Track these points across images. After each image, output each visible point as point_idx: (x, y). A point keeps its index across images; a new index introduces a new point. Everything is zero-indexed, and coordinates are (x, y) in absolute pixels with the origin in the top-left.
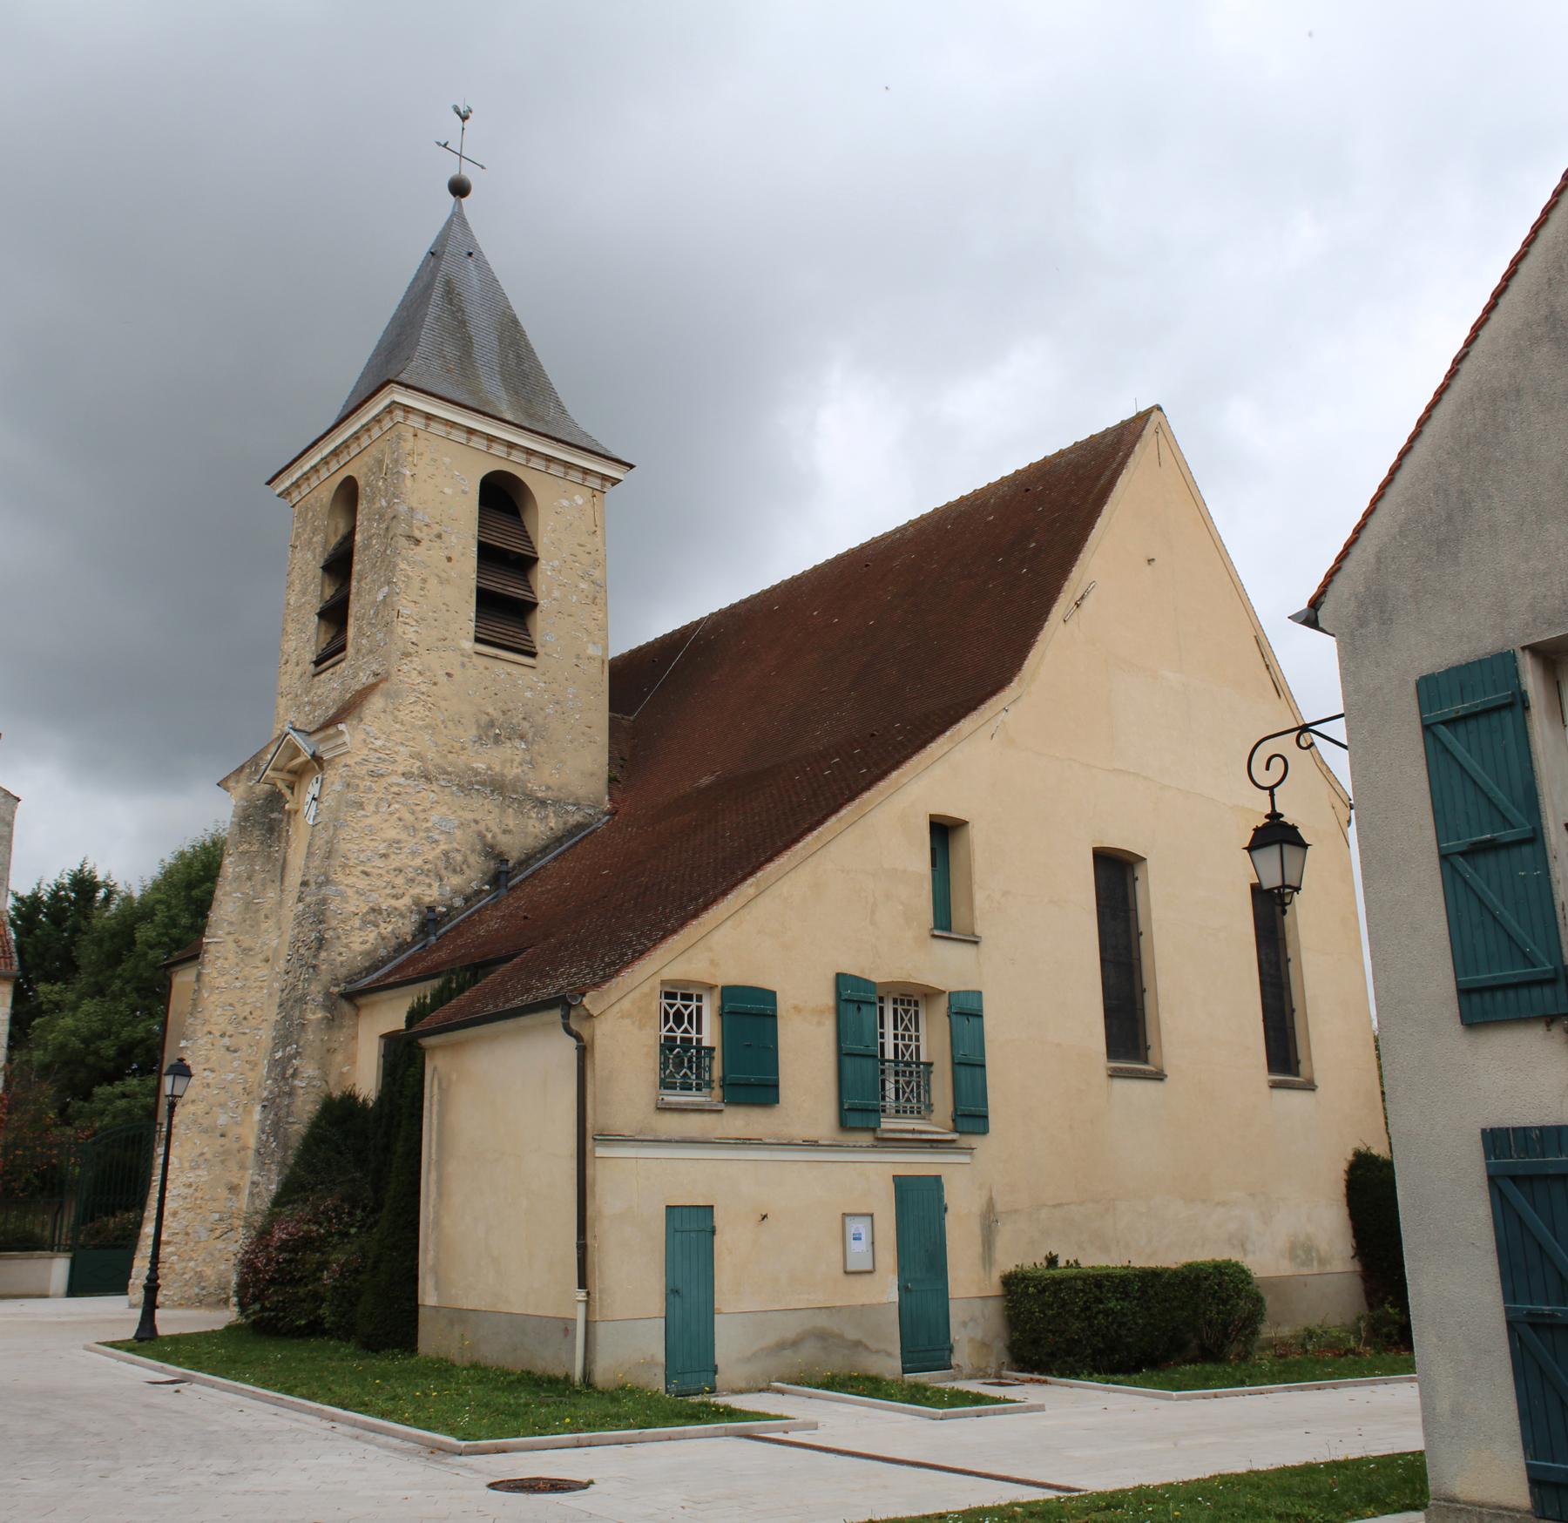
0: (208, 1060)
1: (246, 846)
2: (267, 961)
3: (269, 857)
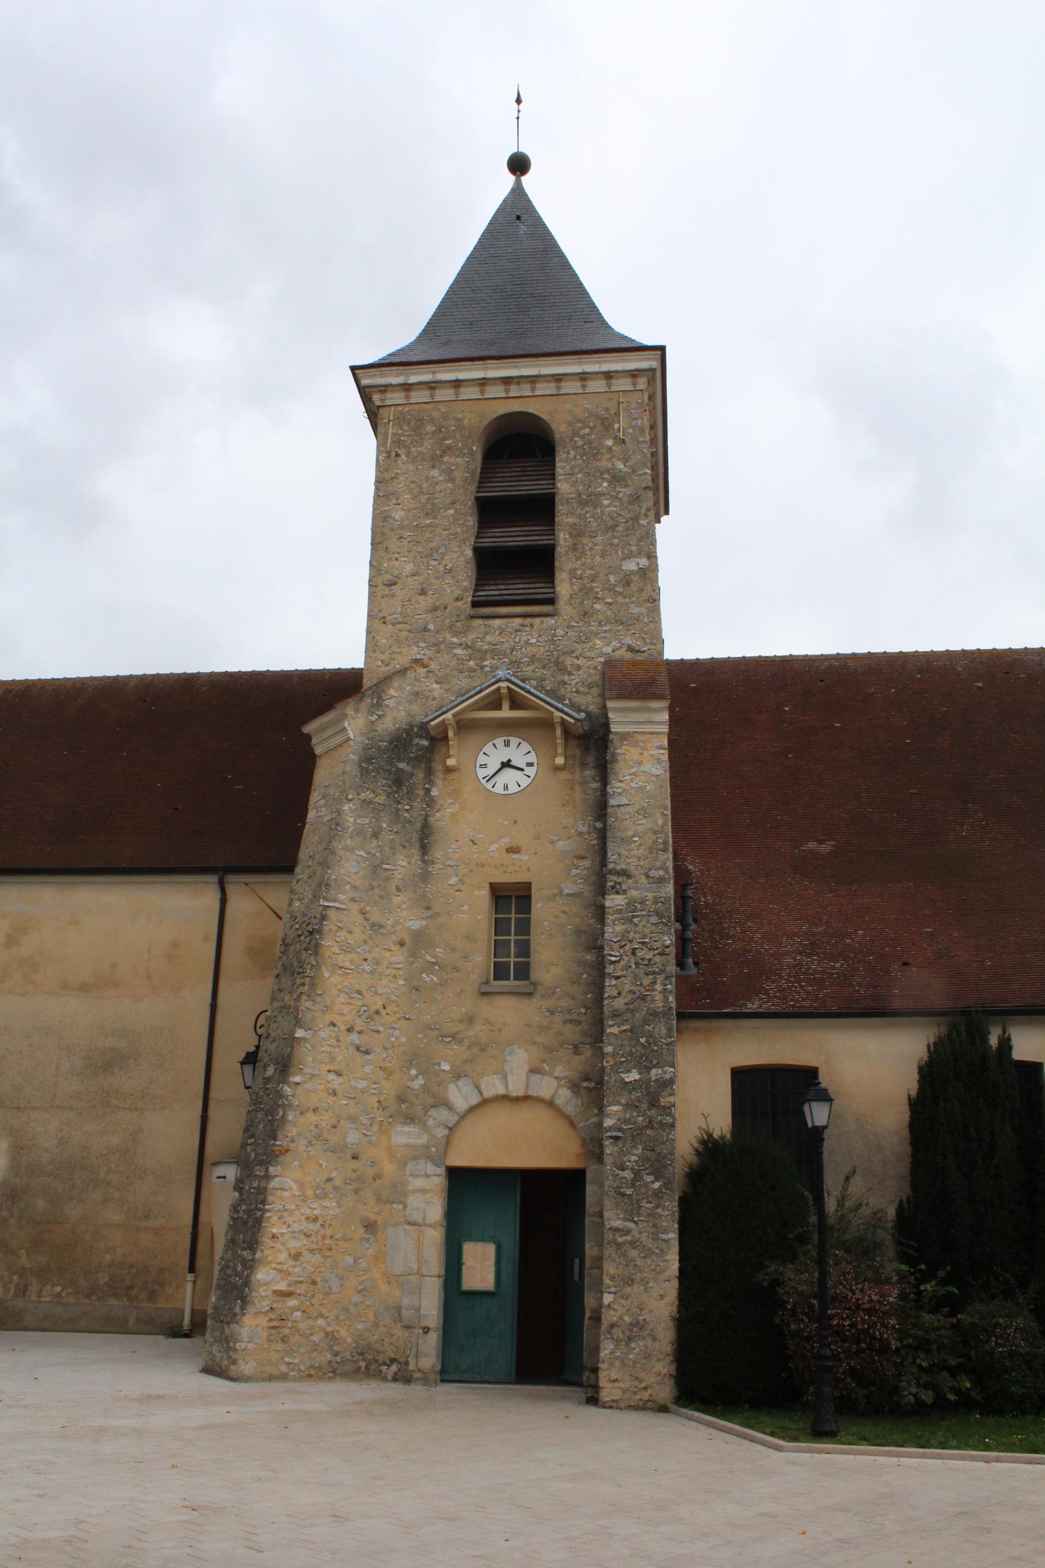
0: (332, 1059)
1: (368, 795)
2: (402, 944)
3: (397, 816)
